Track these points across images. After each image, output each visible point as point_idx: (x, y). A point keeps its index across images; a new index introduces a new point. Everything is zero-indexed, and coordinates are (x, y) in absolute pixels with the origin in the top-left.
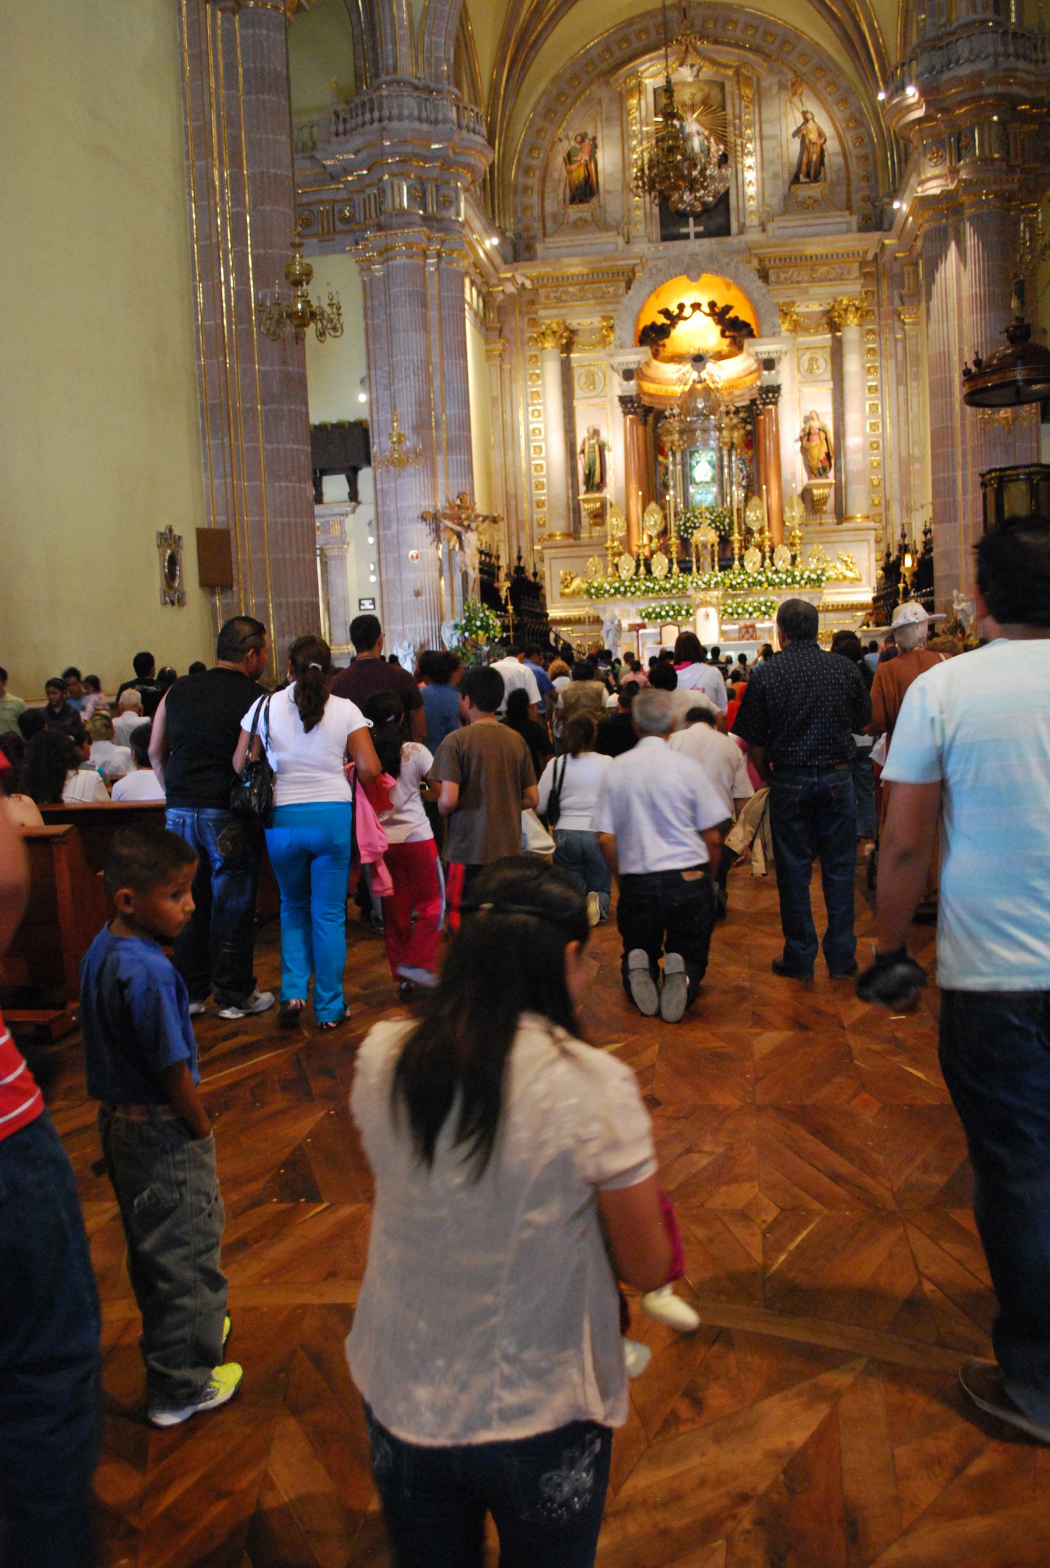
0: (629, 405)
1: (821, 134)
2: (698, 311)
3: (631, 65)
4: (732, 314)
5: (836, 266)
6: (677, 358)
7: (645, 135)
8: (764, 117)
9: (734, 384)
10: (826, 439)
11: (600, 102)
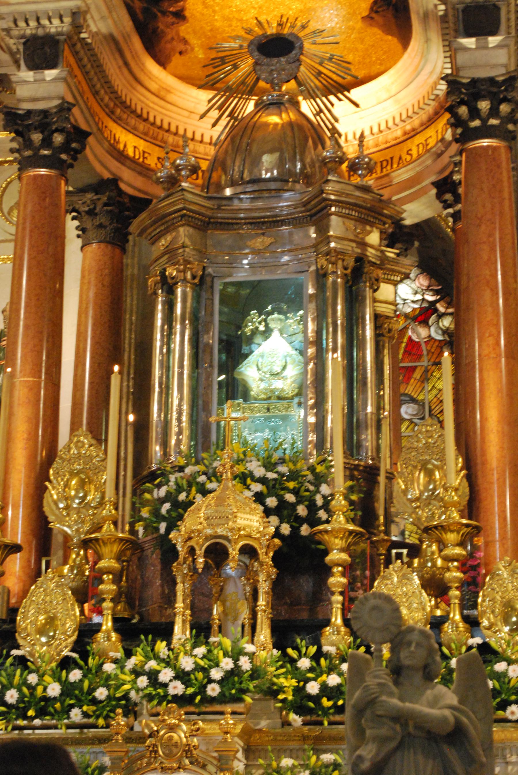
0: (37, 137)
9: (395, 153)
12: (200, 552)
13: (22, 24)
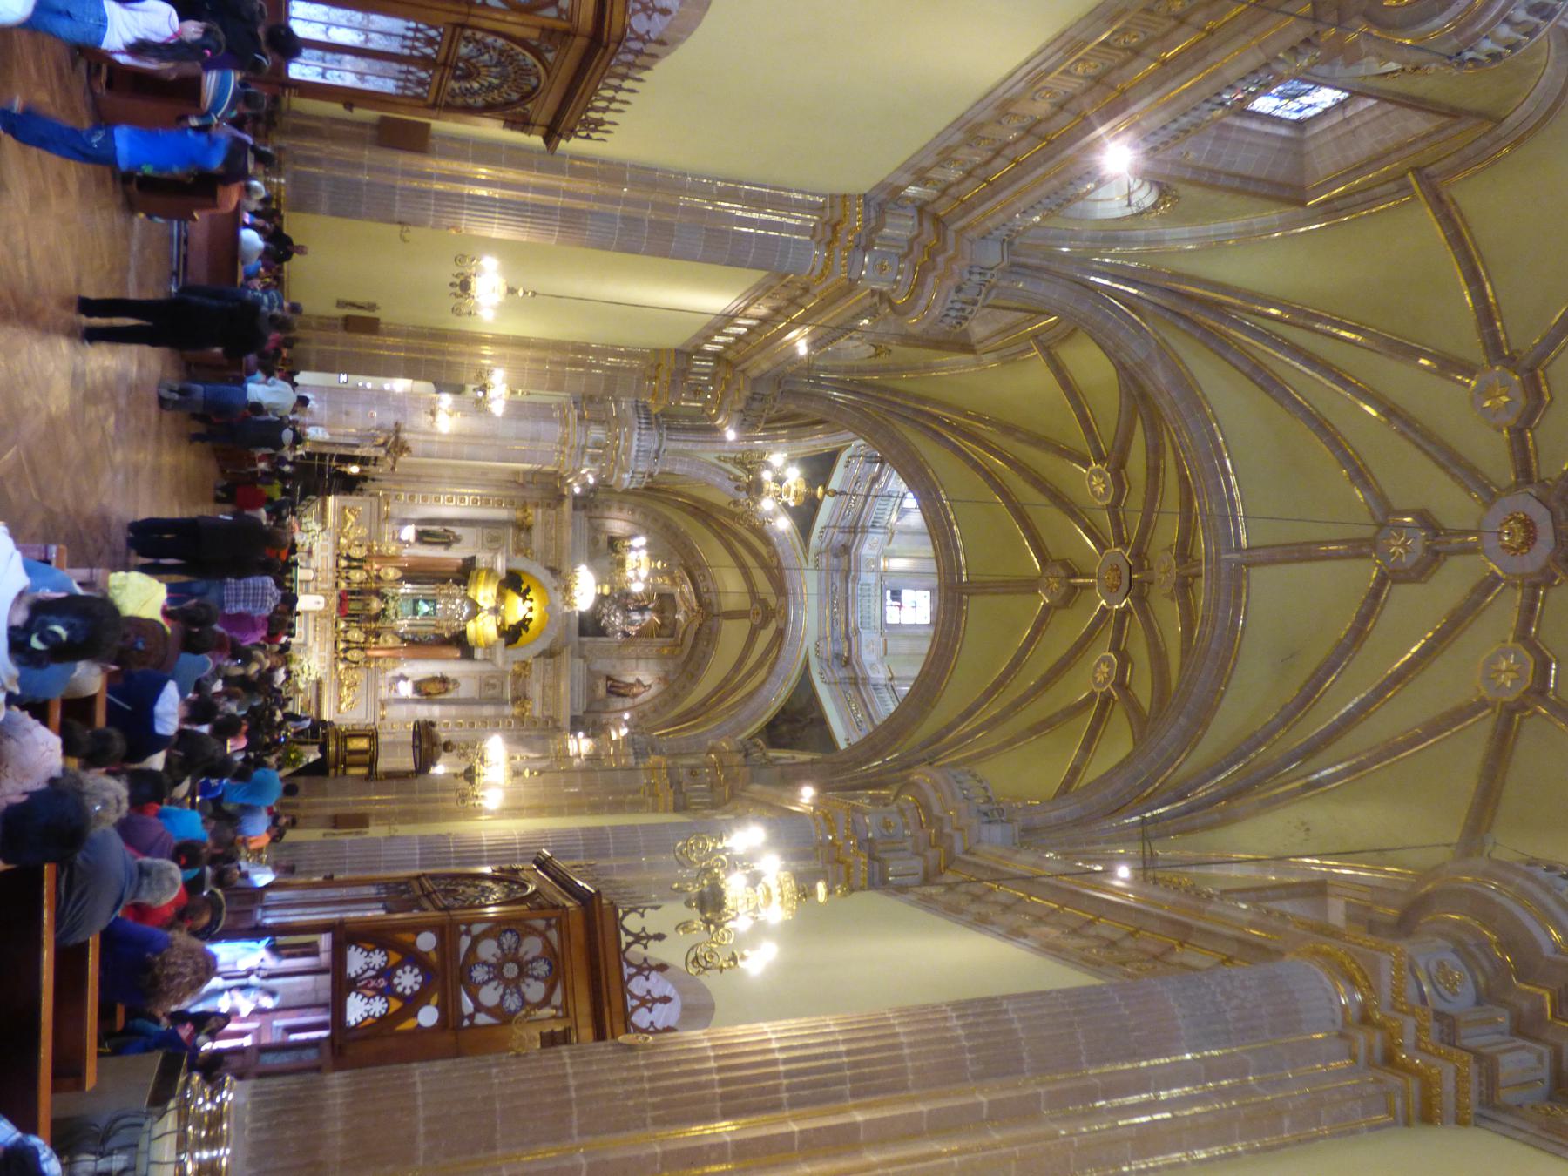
1: (635, 696)
4: (523, 632)
6: (501, 596)
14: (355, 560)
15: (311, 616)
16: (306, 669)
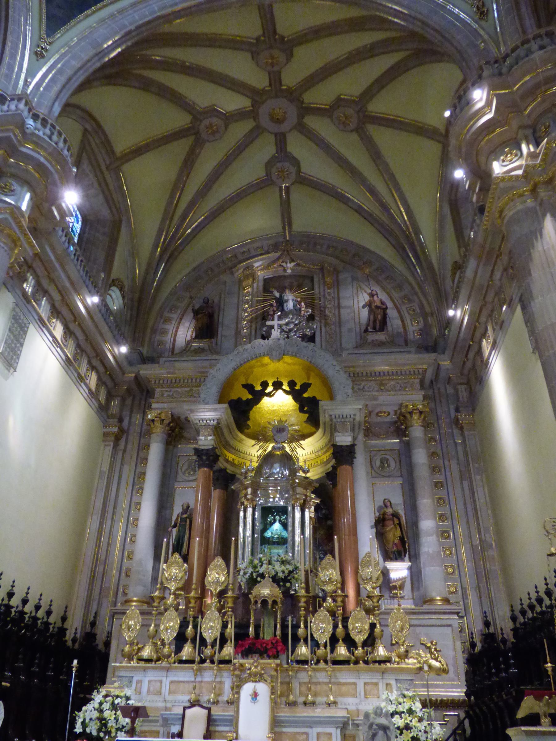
0: (204, 458)
1: (383, 303)
2: (280, 391)
3: (249, 261)
5: (400, 382)
7: (255, 302)
8: (341, 295)
10: (400, 524)
11: (225, 283)
12: (259, 602)
13: (201, 422)
14: (184, 625)
15: (285, 713)
16: (398, 721)
